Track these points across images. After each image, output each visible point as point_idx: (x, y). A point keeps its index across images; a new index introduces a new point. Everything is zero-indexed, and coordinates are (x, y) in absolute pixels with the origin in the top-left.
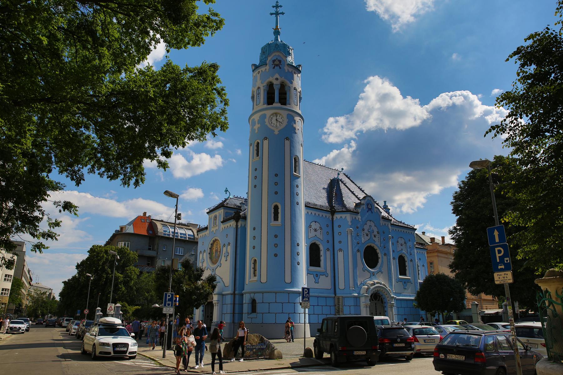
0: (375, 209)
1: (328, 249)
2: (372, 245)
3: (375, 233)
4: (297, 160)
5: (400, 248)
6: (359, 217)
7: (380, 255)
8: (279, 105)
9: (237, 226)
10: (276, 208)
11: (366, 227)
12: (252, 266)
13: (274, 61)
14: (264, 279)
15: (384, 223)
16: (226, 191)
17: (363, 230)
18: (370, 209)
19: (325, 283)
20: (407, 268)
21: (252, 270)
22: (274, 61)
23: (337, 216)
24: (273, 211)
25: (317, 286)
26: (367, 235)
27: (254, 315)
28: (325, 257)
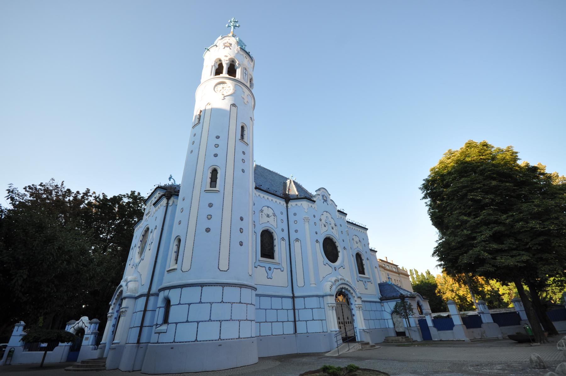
0: (331, 202)
1: (283, 239)
2: (332, 237)
3: (333, 225)
4: (246, 129)
5: (355, 246)
6: (314, 205)
7: (339, 249)
8: (227, 76)
9: (168, 203)
10: (214, 172)
11: (323, 218)
12: (175, 248)
13: (224, 44)
14: (186, 267)
15: (340, 216)
16: (170, 178)
17: (321, 220)
18: (325, 201)
19: (280, 279)
20: (365, 267)
21: (174, 255)
22: (224, 44)
23: (292, 204)
24: (210, 175)
25: (269, 282)
26: (325, 226)
27: (164, 327)
28: (280, 248)
